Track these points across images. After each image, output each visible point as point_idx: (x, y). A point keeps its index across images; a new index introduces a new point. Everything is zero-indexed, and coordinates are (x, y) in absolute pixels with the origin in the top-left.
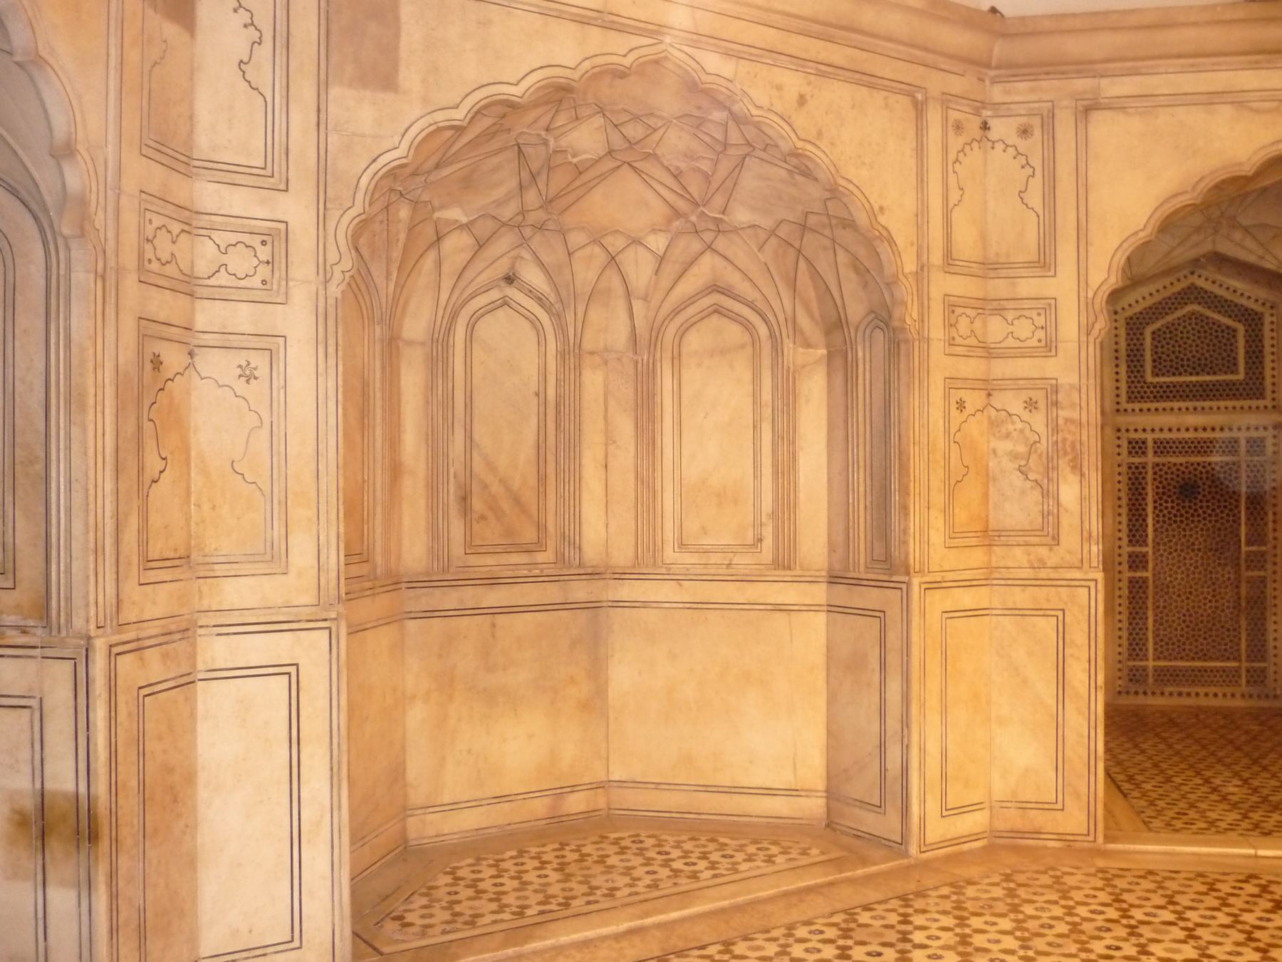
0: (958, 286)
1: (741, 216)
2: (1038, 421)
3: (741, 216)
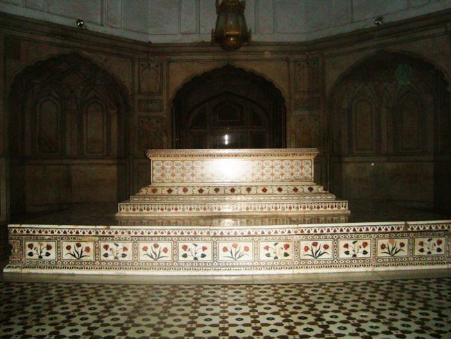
0: (141, 97)
1: (98, 82)
2: (159, 125)
3: (98, 82)
